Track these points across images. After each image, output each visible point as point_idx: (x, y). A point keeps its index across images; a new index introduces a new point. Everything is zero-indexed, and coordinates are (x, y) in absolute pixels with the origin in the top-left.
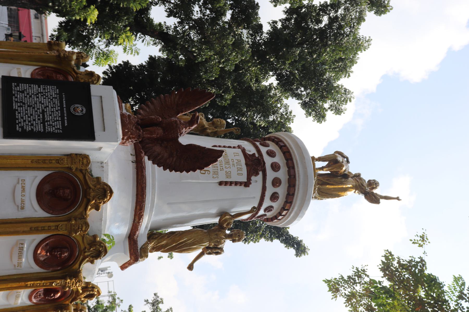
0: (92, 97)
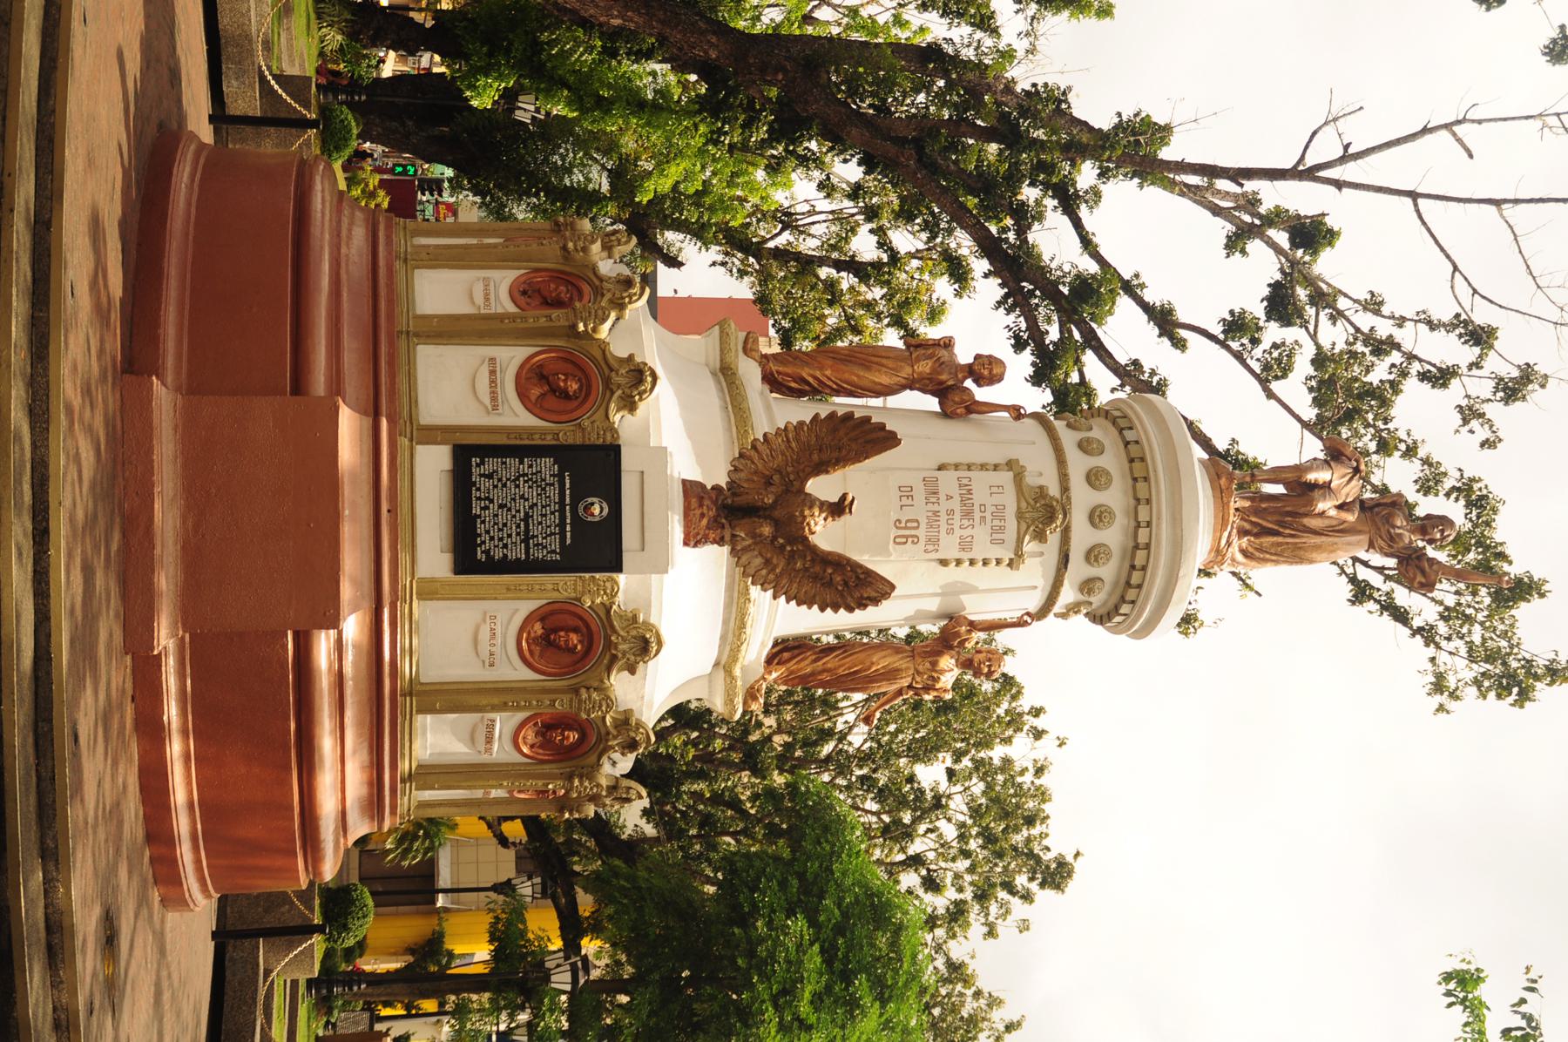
0: (623, 474)
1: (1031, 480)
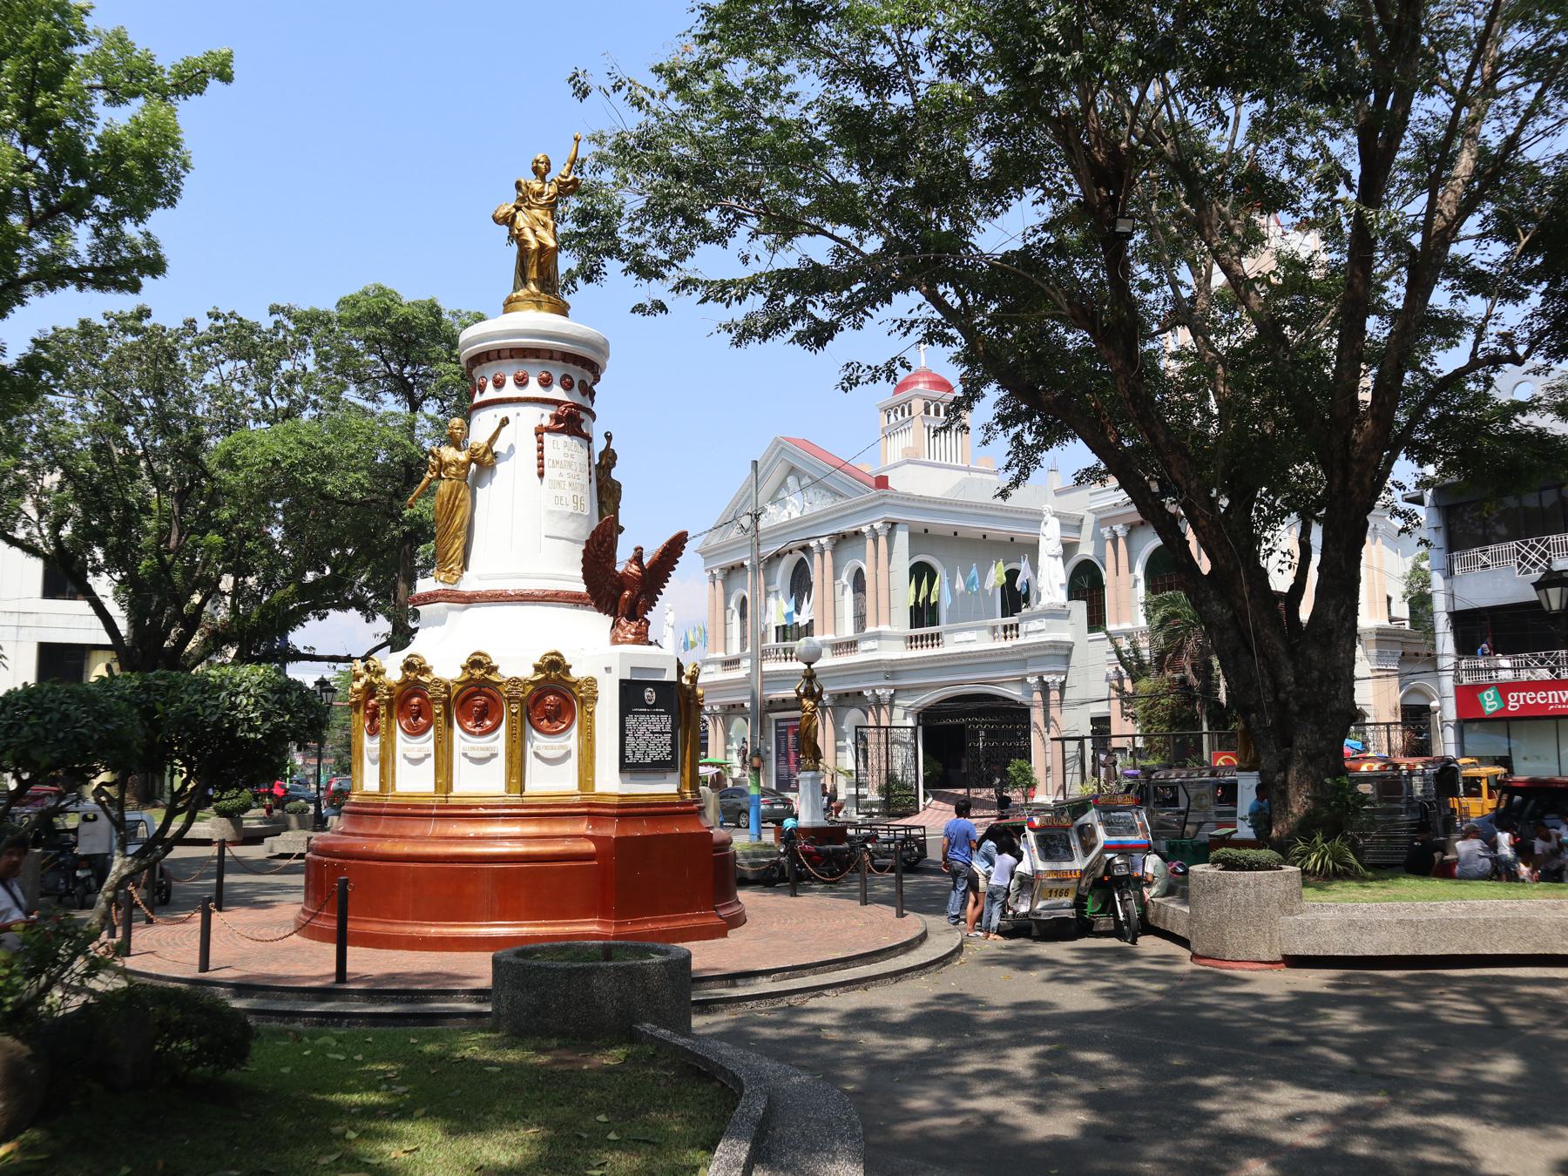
1: (546, 422)
